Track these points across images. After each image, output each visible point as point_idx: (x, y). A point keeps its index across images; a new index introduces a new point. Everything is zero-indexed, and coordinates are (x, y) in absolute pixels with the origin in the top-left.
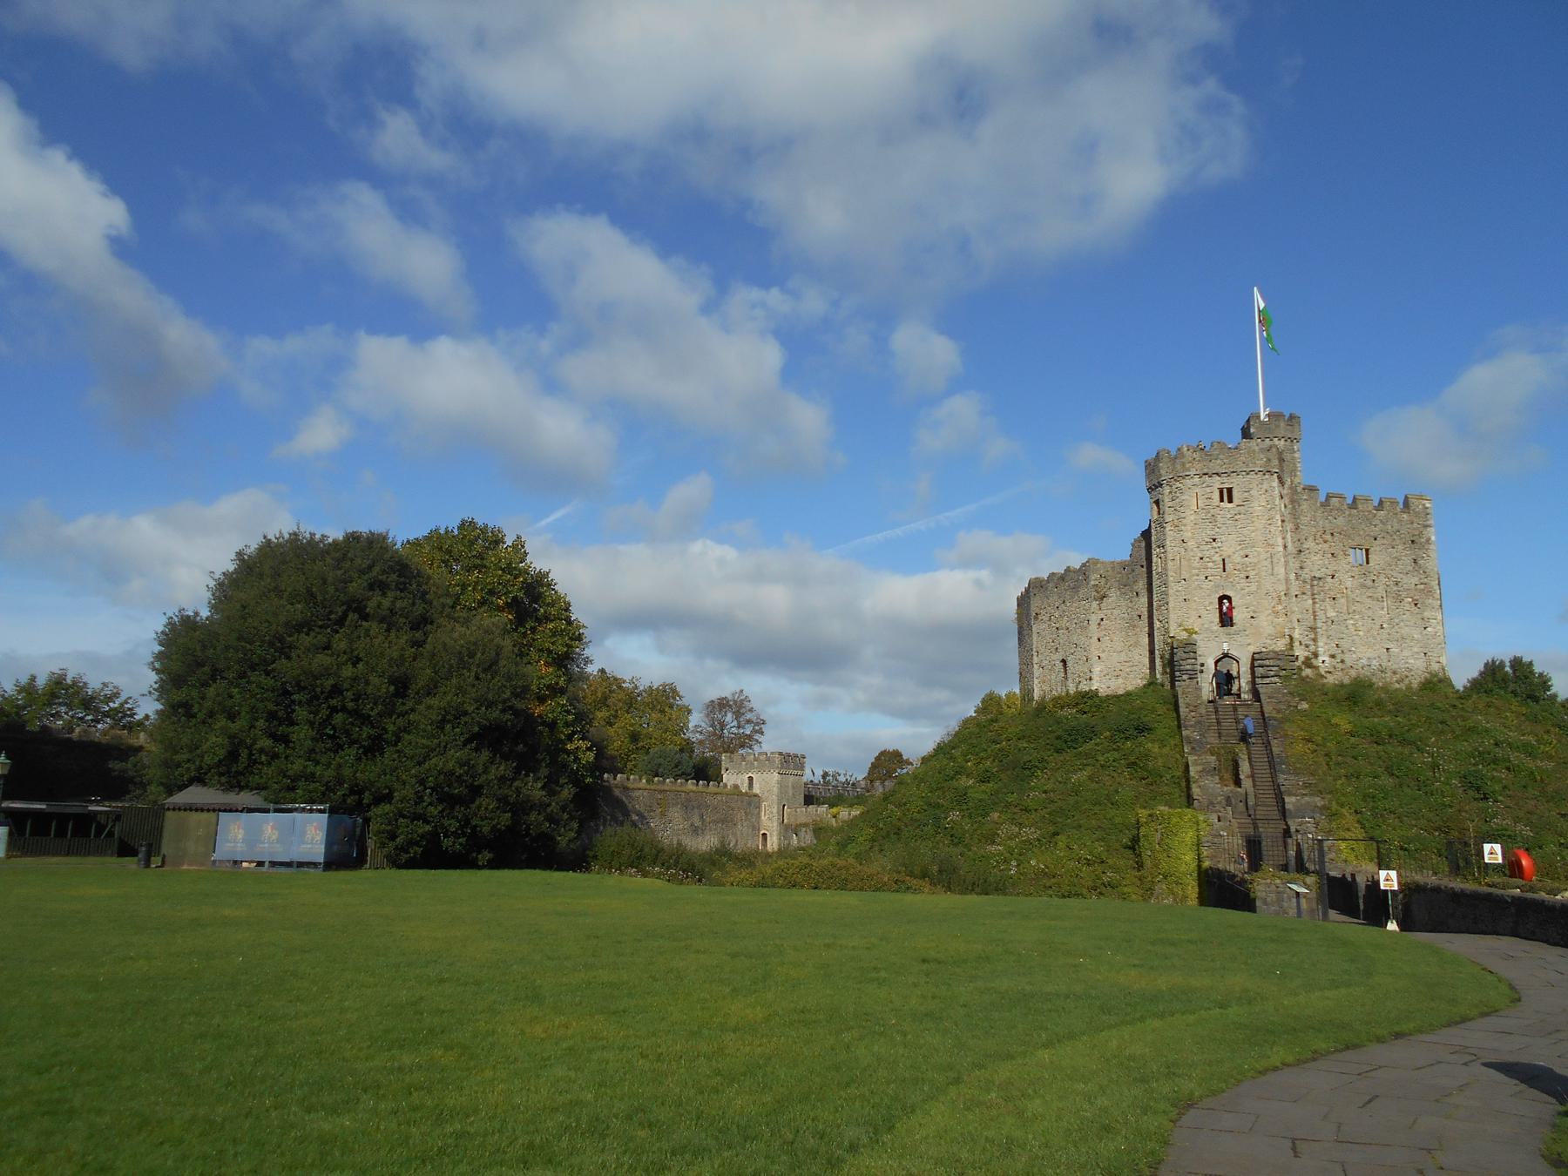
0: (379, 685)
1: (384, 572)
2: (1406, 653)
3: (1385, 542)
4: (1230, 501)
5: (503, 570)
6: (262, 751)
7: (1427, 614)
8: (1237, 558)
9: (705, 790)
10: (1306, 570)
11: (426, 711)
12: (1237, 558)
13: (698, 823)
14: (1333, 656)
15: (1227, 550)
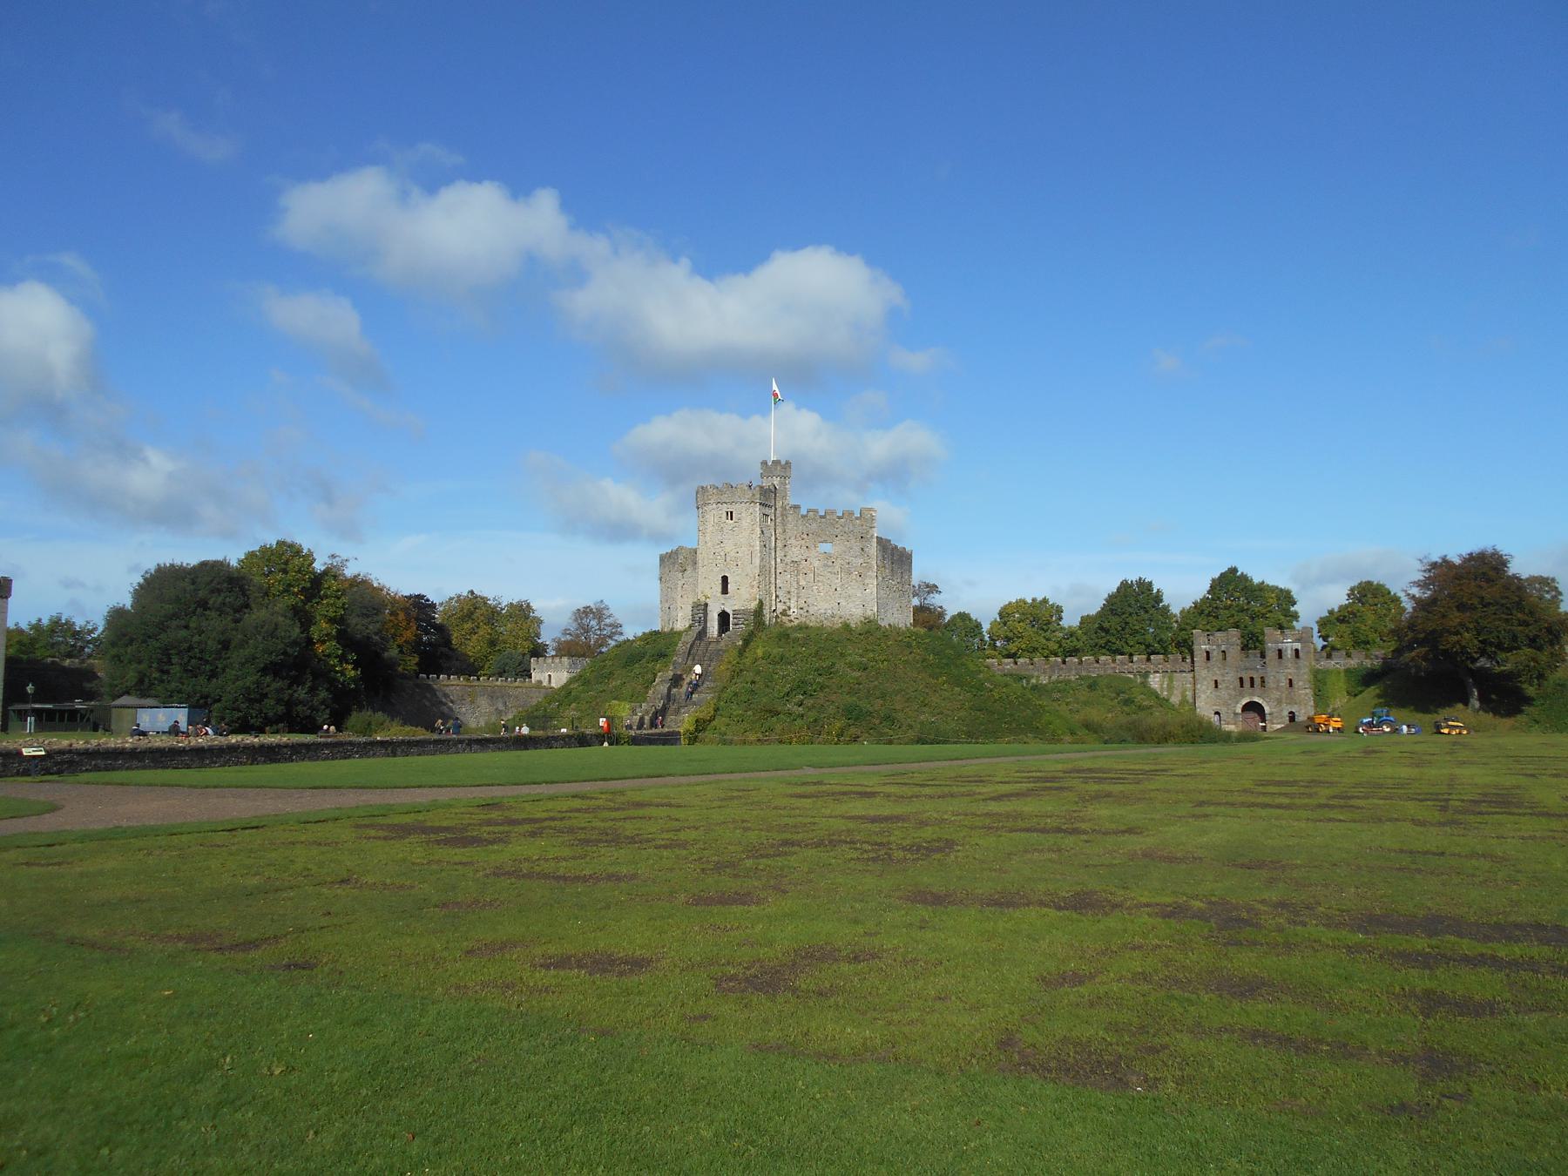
0: (212, 645)
1: (219, 583)
2: (851, 605)
3: (843, 538)
4: (732, 519)
5: (295, 572)
6: (155, 678)
7: (866, 582)
8: (733, 554)
9: (505, 684)
10: (788, 557)
11: (236, 656)
12: (733, 554)
13: (501, 707)
14: (802, 609)
15: (728, 549)
